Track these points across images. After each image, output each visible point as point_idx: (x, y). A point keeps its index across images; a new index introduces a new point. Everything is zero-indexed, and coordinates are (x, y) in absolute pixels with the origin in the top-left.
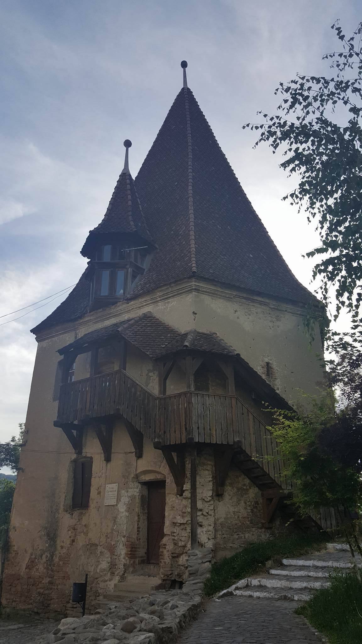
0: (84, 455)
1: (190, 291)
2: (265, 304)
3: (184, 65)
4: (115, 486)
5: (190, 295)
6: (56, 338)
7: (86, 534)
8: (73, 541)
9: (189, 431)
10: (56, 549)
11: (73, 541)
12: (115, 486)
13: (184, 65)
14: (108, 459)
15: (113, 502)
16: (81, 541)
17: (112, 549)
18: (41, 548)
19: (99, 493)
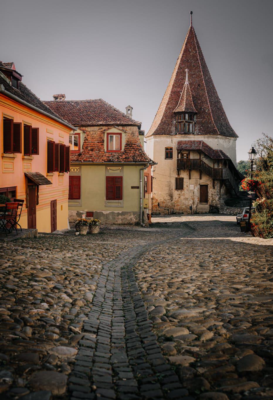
0: (180, 176)
1: (217, 138)
2: (228, 139)
3: (191, 13)
4: (193, 185)
5: (216, 139)
6: (163, 139)
7: (184, 196)
8: (179, 197)
9: (222, 177)
10: (173, 199)
11: (179, 197)
12: (193, 185)
13: (191, 13)
14: (190, 178)
15: (193, 189)
16: (182, 197)
17: (193, 199)
18: (167, 198)
19: (187, 186)
